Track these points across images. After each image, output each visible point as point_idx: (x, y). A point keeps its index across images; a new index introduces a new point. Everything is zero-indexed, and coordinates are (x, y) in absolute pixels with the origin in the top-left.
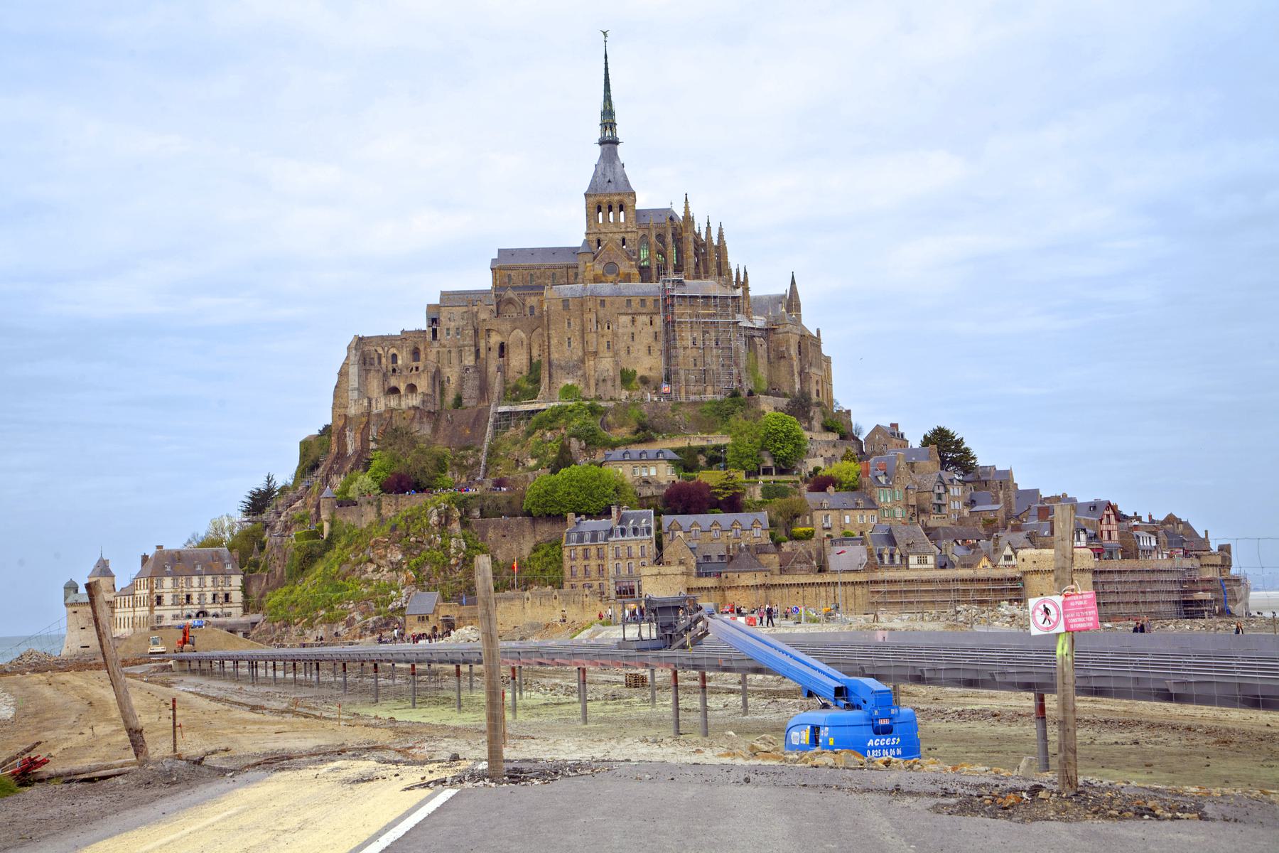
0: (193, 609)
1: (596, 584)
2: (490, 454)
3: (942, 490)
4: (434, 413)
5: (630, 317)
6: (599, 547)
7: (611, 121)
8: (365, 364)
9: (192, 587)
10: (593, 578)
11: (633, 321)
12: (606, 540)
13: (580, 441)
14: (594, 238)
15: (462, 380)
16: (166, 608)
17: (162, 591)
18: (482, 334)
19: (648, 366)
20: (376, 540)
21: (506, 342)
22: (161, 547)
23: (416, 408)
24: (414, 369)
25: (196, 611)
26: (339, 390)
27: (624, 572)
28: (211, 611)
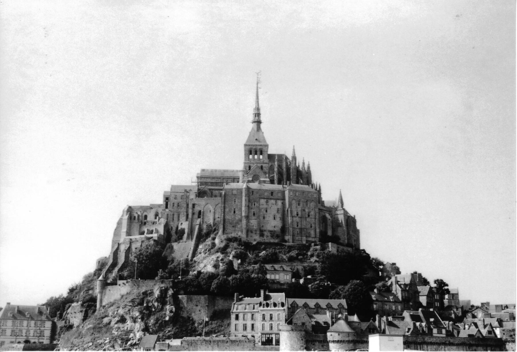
0: (22, 339)
3: (431, 295)
5: (266, 200)
6: (253, 313)
7: (258, 112)
11: (267, 202)
12: (257, 308)
13: (238, 260)
14: (248, 165)
16: (7, 337)
17: (6, 327)
18: (190, 206)
19: (274, 225)
21: (202, 211)
25: (24, 340)
26: (117, 233)
27: (267, 330)
28: (32, 341)
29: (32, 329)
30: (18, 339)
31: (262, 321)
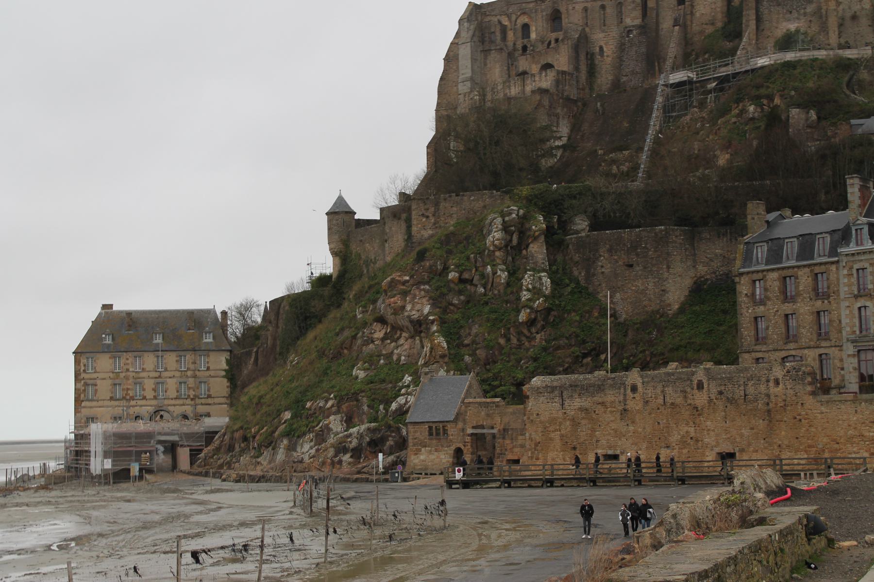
1: (811, 356)
2: (655, 153)
4: (575, 102)
6: (817, 270)
8: (483, 42)
9: (144, 370)
10: (804, 341)
12: (833, 252)
13: (808, 113)
15: (621, 47)
16: (100, 403)
17: (95, 376)
20: (393, 279)
22: (111, 306)
23: (543, 91)
24: (553, 42)
25: (151, 409)
29: (170, 378)
30: (133, 406)
31: (856, 297)
